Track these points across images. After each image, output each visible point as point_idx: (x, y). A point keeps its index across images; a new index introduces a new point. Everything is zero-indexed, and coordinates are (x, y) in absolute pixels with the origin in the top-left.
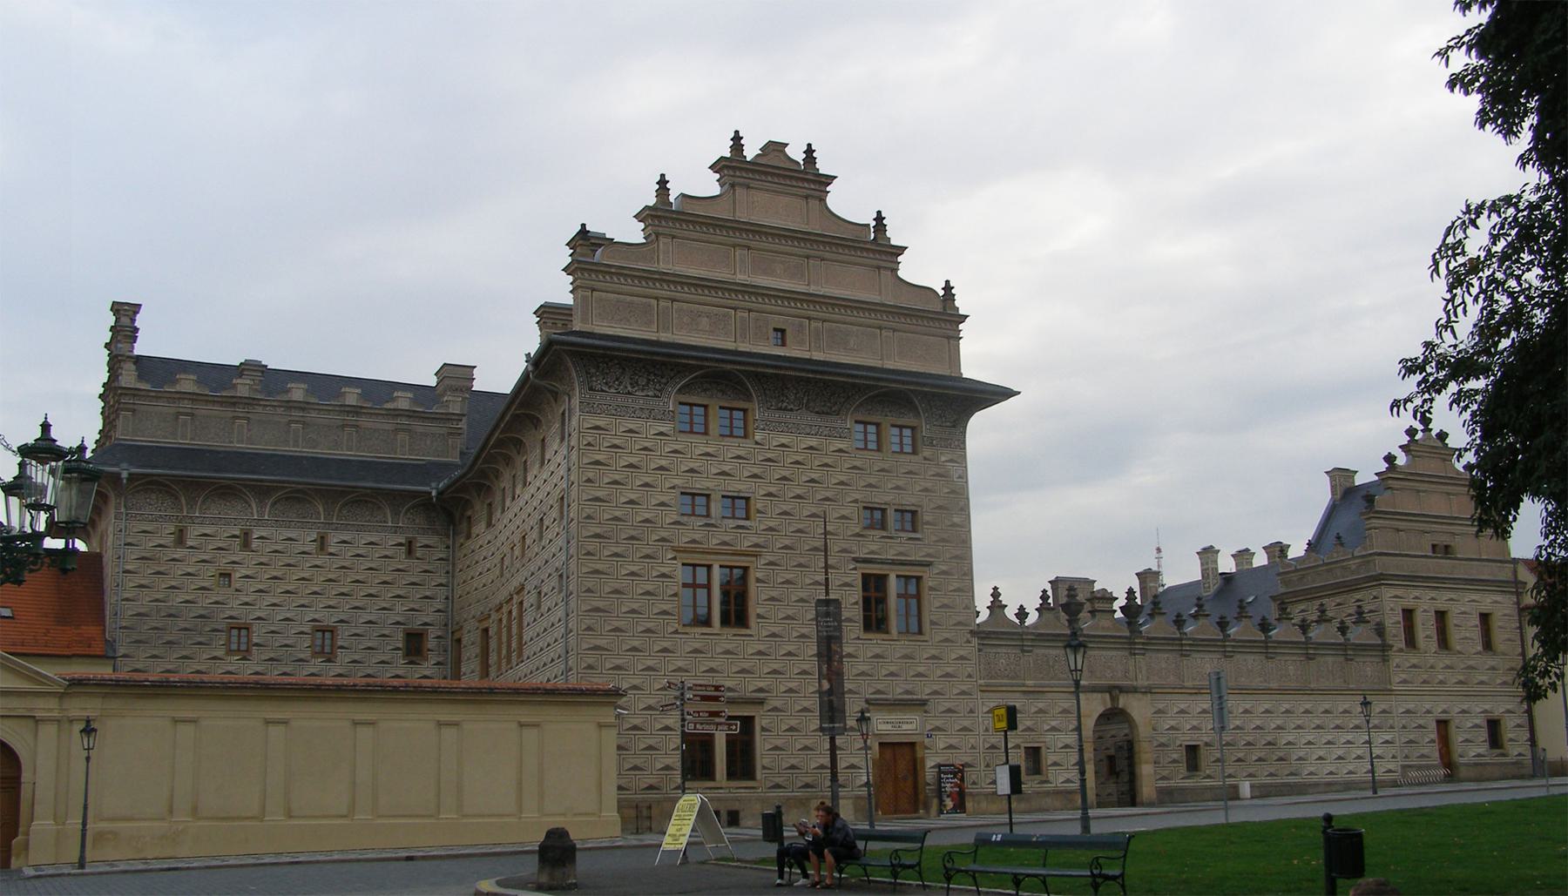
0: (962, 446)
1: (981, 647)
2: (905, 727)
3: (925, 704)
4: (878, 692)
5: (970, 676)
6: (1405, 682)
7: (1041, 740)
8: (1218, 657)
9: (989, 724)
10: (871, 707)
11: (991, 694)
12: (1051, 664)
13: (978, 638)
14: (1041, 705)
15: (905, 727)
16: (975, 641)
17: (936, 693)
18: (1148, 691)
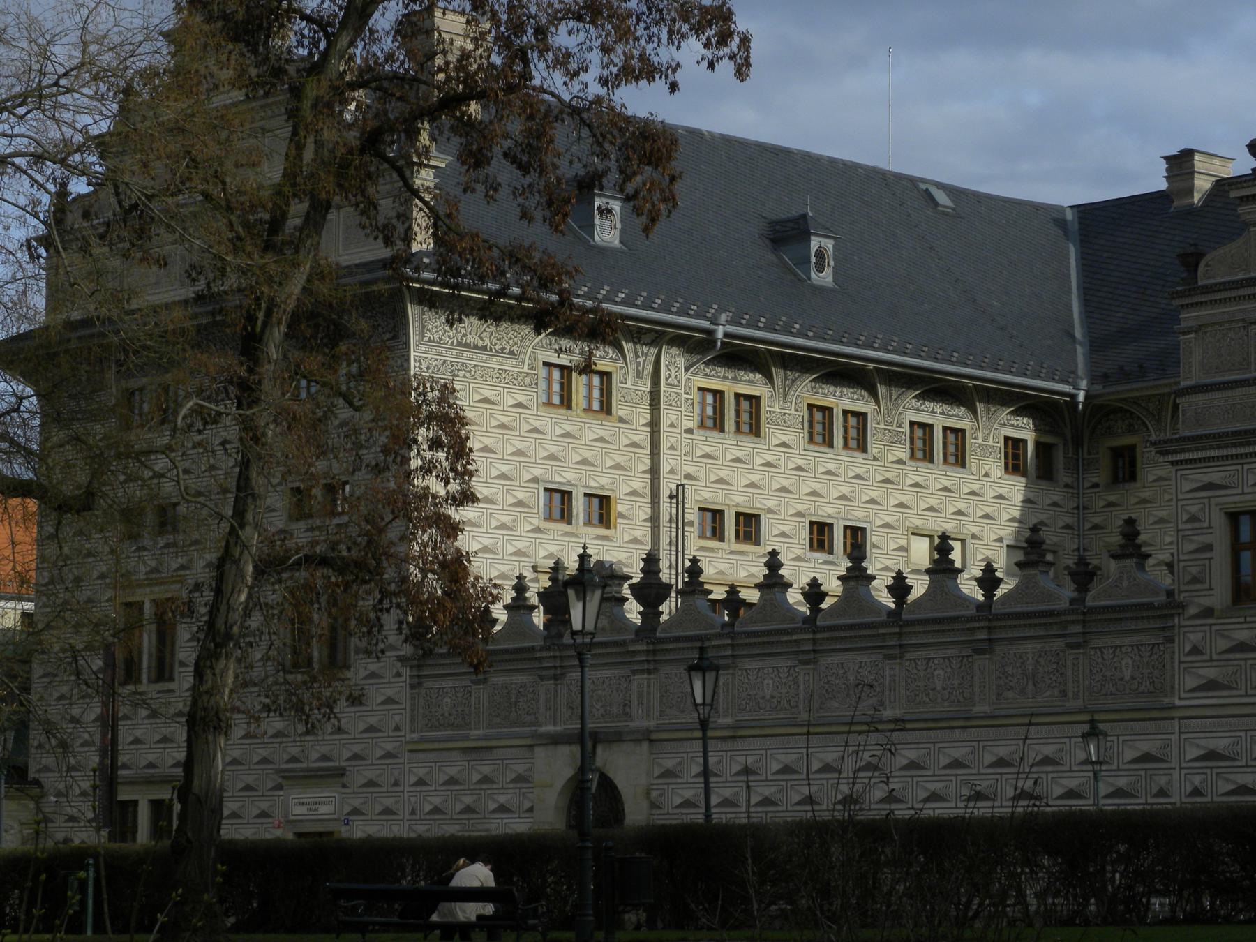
0: (405, 365)
1: (416, 680)
2: (323, 809)
3: (343, 775)
4: (294, 759)
5: (397, 728)
6: (1211, 685)
7: (487, 826)
8: (789, 663)
9: (416, 802)
10: (284, 783)
11: (421, 756)
12: (513, 700)
13: (411, 667)
14: (486, 770)
15: (323, 809)
16: (406, 672)
17: (356, 757)
18: (647, 737)
